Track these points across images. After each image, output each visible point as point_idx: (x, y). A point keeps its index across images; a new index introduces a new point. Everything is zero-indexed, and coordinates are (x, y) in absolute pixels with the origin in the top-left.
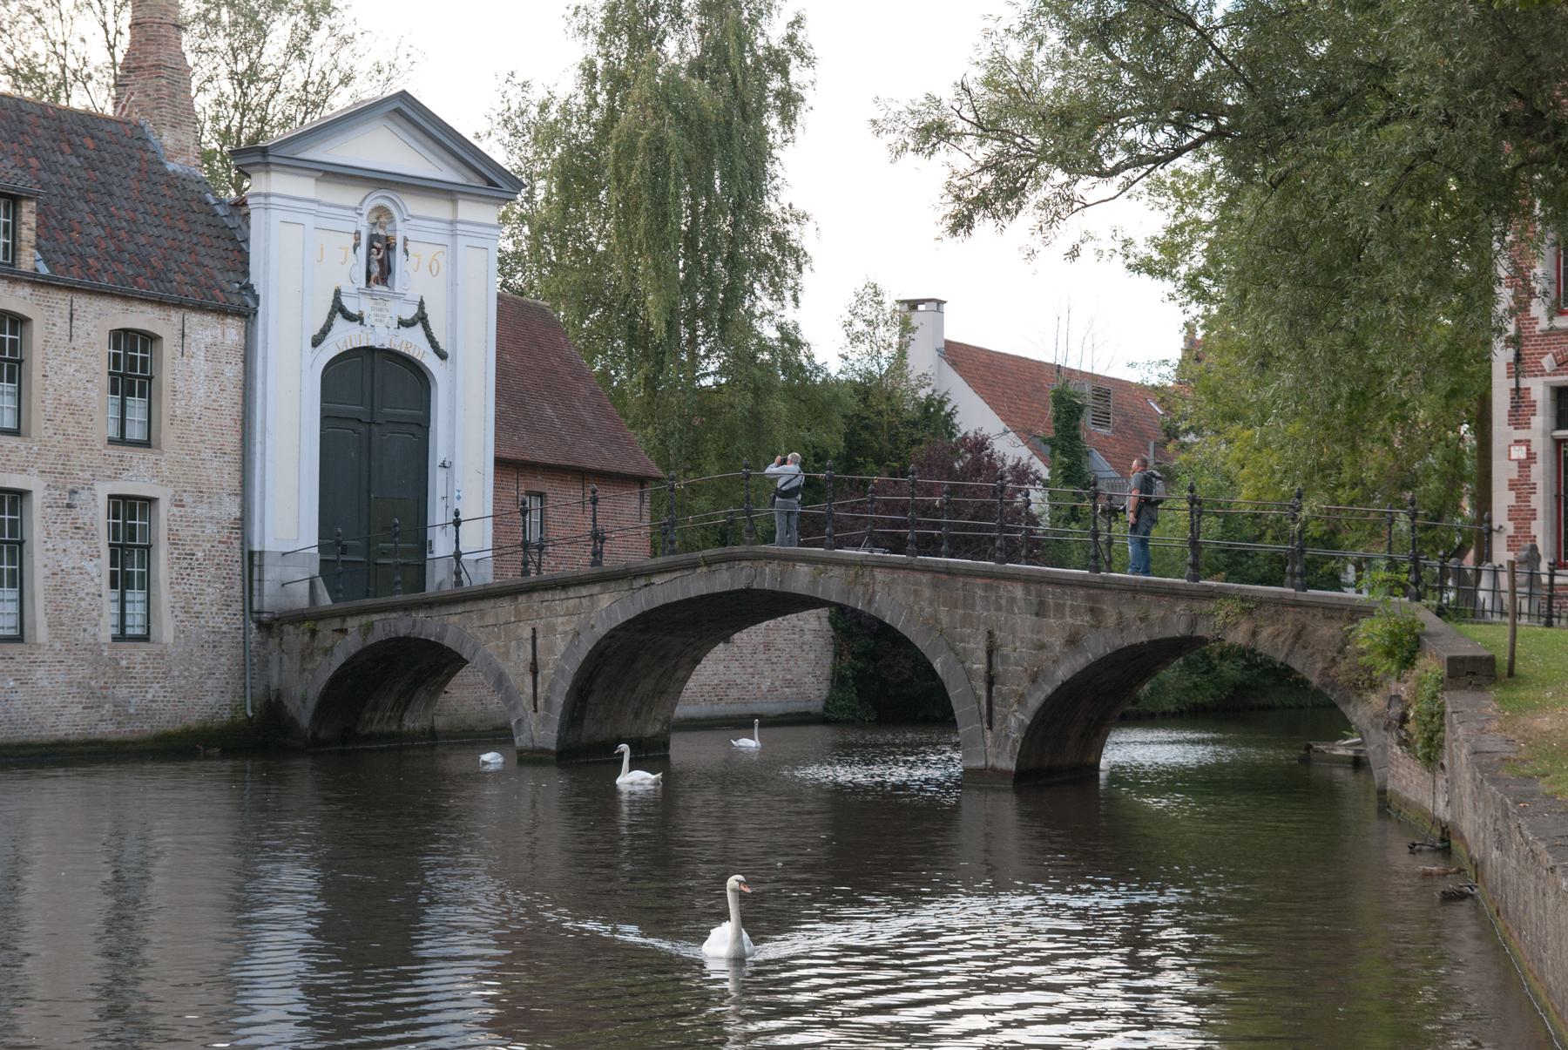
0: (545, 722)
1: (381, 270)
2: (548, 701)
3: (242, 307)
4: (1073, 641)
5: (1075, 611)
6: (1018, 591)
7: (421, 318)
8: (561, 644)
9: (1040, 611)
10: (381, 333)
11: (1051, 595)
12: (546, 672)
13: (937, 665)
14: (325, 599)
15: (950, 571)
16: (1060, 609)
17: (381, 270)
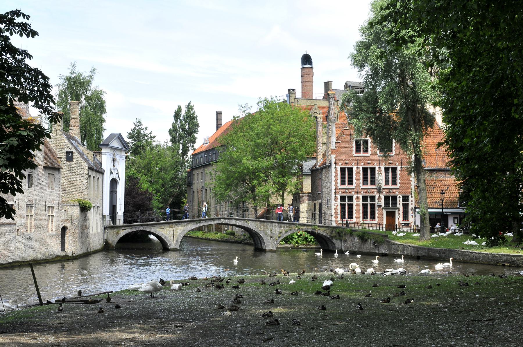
0: (176, 244)
1: (114, 166)
2: (177, 241)
3: (101, 172)
4: (286, 232)
5: (287, 227)
6: (277, 224)
7: (117, 174)
8: (179, 232)
9: (281, 227)
10: (115, 176)
11: (282, 225)
12: (176, 236)
13: (261, 235)
14: (112, 224)
15: (264, 222)
16: (284, 227)
17: (114, 166)
